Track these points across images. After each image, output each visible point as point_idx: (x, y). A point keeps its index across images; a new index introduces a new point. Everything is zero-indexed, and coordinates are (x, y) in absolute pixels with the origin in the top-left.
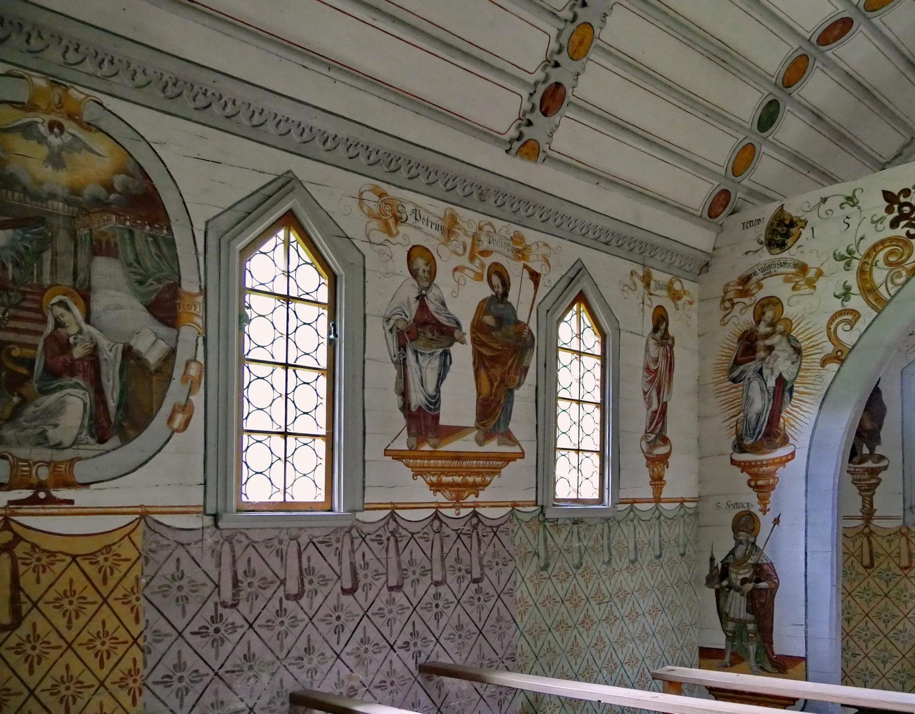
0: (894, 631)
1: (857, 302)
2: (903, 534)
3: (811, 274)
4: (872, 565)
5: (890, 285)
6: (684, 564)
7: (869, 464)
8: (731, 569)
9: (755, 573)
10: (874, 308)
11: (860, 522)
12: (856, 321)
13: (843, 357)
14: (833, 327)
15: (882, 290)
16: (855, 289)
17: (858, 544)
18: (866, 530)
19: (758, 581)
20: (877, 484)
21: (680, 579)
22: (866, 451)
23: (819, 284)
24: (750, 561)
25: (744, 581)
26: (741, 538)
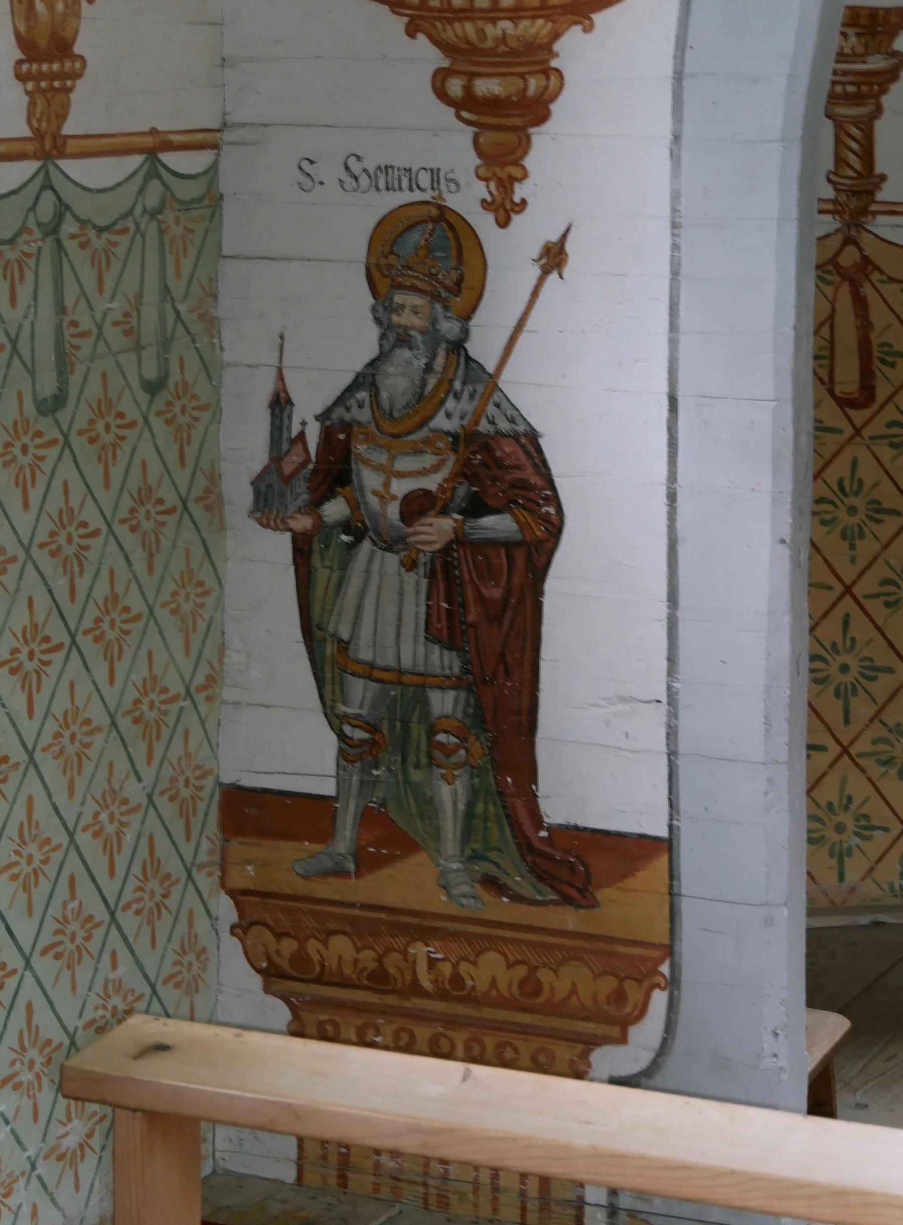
4: (866, 394)
6: (158, 424)
8: (361, 448)
9: (465, 473)
18: (849, 257)
19: (477, 507)
21: (145, 494)
24: (440, 422)
25: (417, 506)
26: (406, 318)
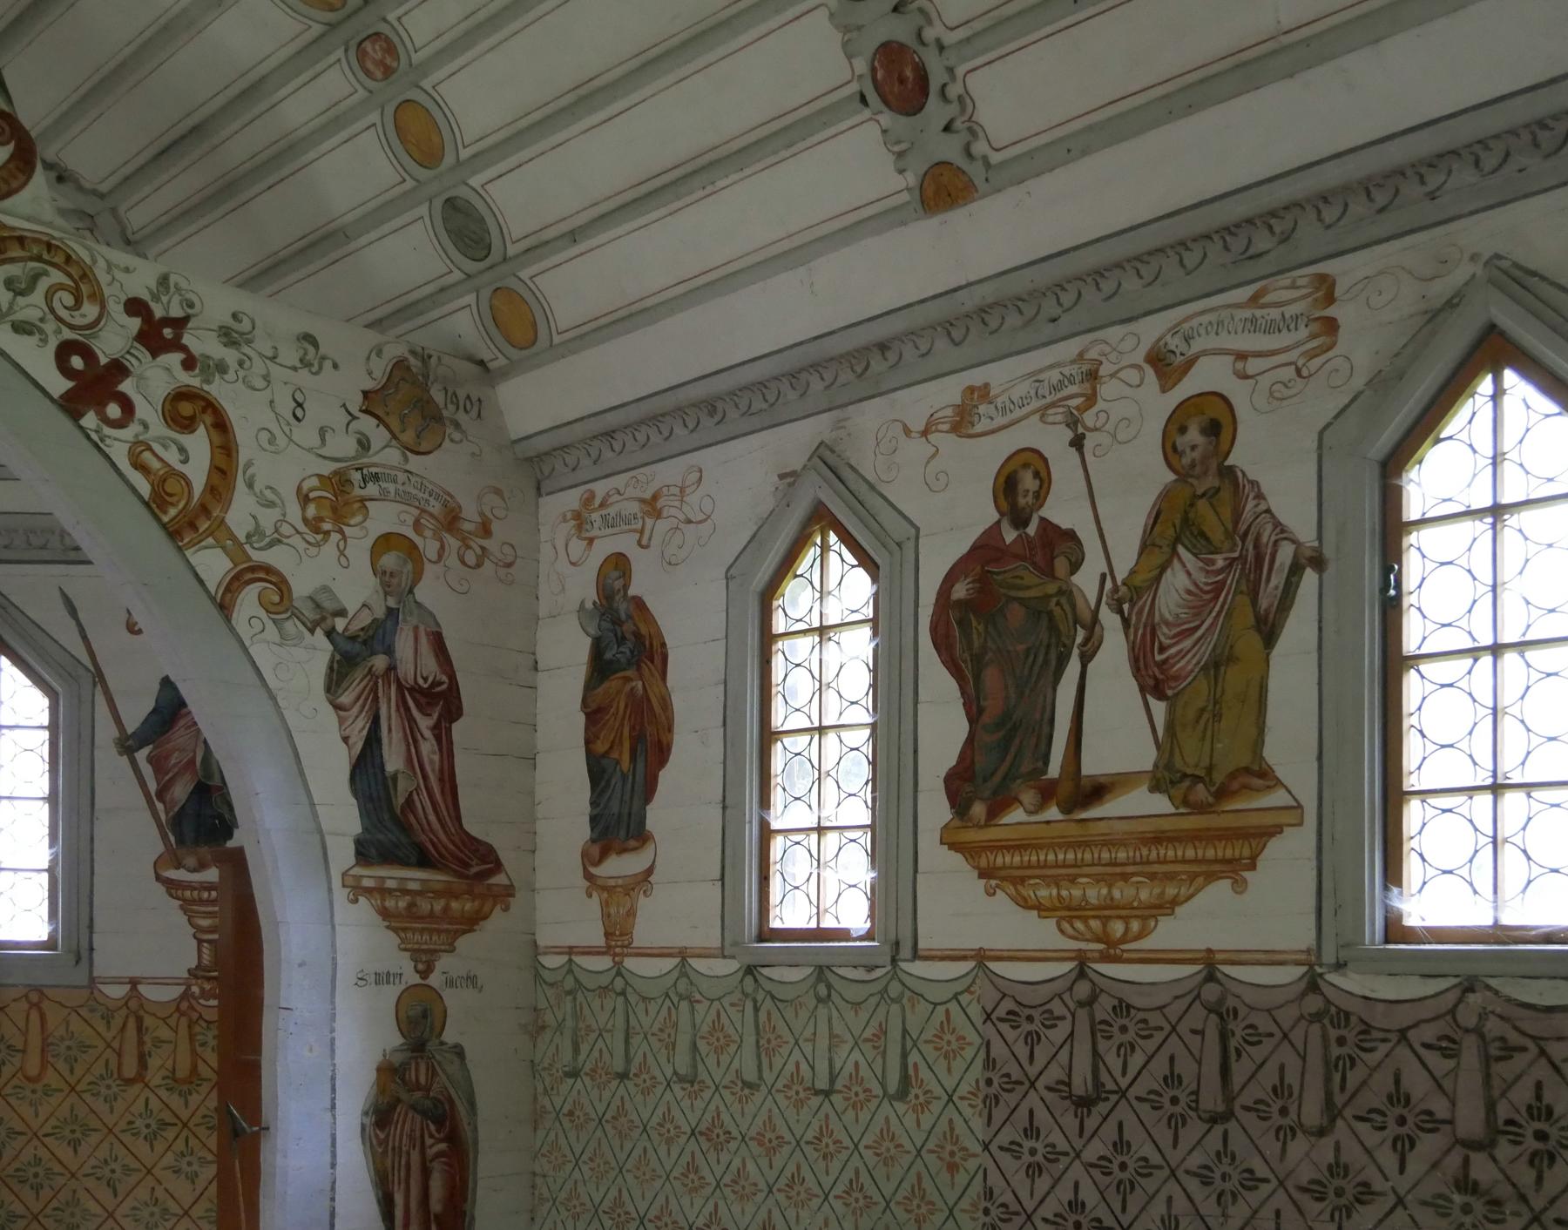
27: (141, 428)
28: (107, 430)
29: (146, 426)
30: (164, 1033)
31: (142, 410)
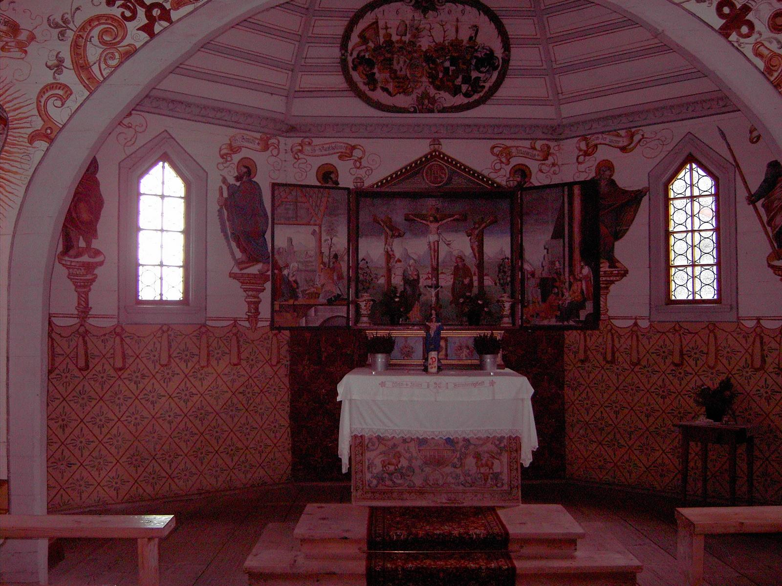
0: (109, 436)
1: (69, 77)
2: (118, 334)
3: (23, 36)
4: (87, 367)
5: (103, 66)
7: (85, 258)
10: (86, 87)
11: (76, 321)
12: (68, 98)
13: (52, 136)
14: (43, 100)
15: (95, 69)
16: (68, 63)
17: (73, 343)
18: (82, 330)
20: (93, 280)
22: (82, 244)
23: (32, 48)
27: (758, 36)
28: (742, 40)
29: (761, 34)
30: (773, 345)
31: (758, 26)
